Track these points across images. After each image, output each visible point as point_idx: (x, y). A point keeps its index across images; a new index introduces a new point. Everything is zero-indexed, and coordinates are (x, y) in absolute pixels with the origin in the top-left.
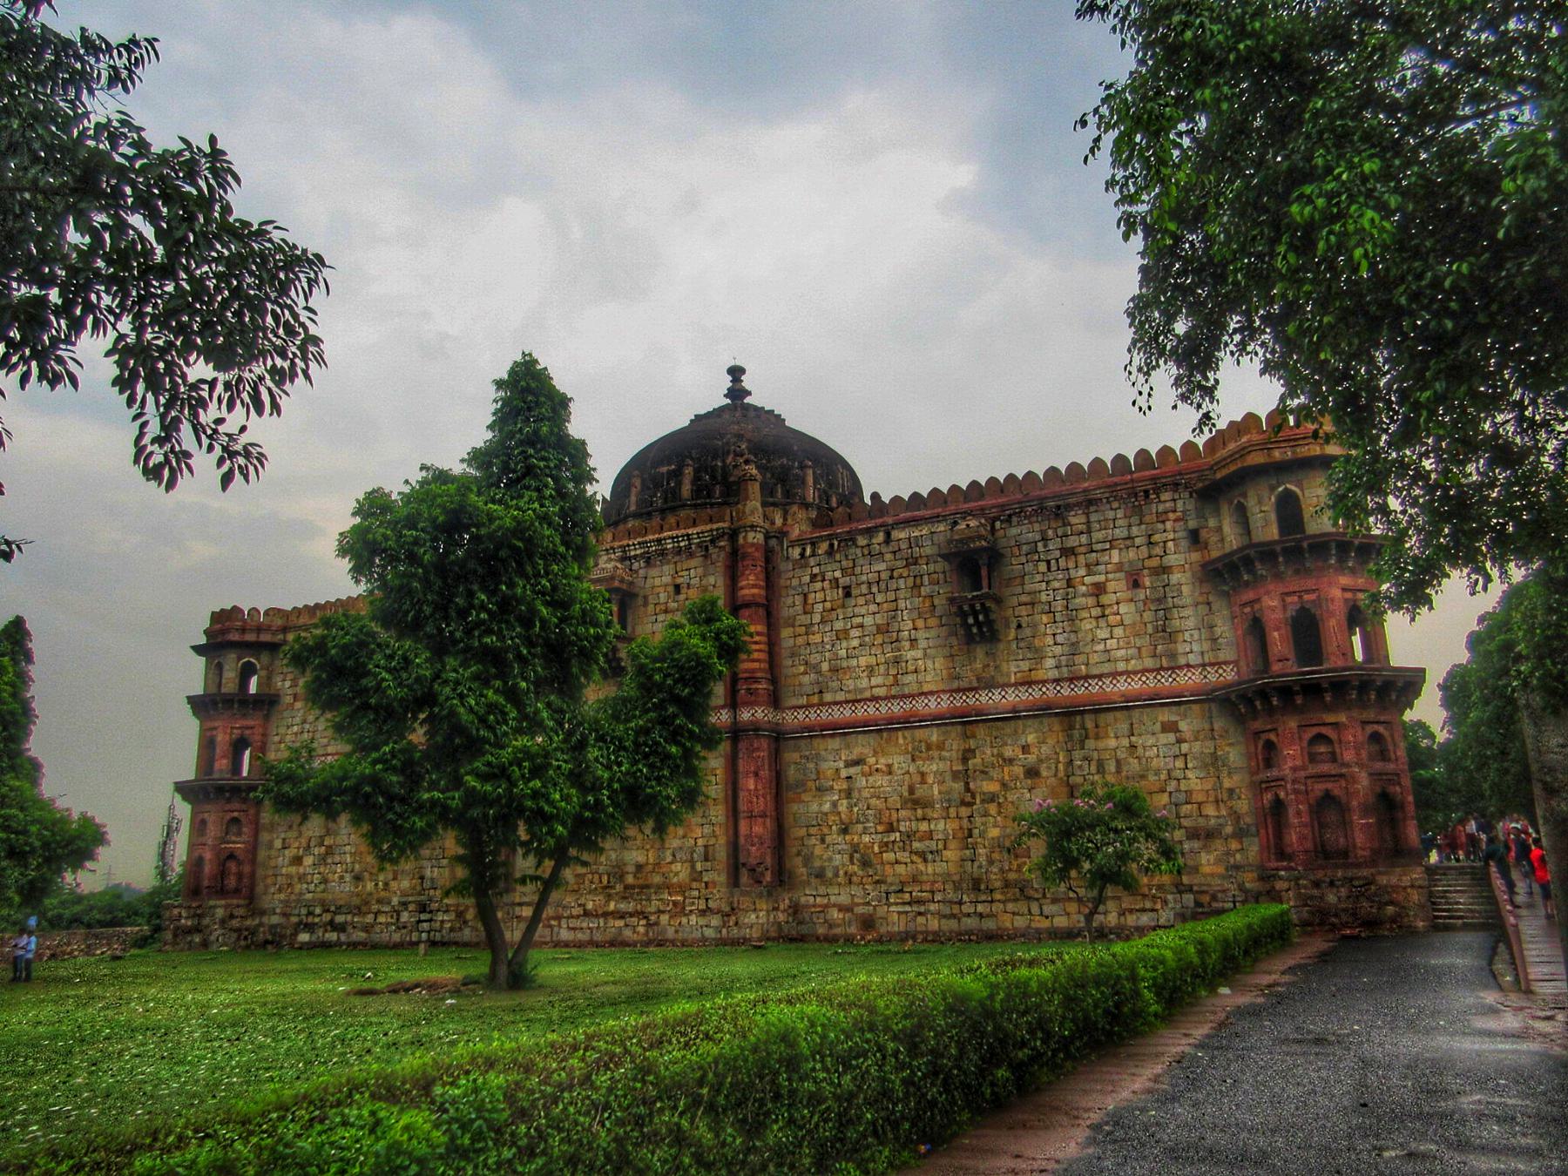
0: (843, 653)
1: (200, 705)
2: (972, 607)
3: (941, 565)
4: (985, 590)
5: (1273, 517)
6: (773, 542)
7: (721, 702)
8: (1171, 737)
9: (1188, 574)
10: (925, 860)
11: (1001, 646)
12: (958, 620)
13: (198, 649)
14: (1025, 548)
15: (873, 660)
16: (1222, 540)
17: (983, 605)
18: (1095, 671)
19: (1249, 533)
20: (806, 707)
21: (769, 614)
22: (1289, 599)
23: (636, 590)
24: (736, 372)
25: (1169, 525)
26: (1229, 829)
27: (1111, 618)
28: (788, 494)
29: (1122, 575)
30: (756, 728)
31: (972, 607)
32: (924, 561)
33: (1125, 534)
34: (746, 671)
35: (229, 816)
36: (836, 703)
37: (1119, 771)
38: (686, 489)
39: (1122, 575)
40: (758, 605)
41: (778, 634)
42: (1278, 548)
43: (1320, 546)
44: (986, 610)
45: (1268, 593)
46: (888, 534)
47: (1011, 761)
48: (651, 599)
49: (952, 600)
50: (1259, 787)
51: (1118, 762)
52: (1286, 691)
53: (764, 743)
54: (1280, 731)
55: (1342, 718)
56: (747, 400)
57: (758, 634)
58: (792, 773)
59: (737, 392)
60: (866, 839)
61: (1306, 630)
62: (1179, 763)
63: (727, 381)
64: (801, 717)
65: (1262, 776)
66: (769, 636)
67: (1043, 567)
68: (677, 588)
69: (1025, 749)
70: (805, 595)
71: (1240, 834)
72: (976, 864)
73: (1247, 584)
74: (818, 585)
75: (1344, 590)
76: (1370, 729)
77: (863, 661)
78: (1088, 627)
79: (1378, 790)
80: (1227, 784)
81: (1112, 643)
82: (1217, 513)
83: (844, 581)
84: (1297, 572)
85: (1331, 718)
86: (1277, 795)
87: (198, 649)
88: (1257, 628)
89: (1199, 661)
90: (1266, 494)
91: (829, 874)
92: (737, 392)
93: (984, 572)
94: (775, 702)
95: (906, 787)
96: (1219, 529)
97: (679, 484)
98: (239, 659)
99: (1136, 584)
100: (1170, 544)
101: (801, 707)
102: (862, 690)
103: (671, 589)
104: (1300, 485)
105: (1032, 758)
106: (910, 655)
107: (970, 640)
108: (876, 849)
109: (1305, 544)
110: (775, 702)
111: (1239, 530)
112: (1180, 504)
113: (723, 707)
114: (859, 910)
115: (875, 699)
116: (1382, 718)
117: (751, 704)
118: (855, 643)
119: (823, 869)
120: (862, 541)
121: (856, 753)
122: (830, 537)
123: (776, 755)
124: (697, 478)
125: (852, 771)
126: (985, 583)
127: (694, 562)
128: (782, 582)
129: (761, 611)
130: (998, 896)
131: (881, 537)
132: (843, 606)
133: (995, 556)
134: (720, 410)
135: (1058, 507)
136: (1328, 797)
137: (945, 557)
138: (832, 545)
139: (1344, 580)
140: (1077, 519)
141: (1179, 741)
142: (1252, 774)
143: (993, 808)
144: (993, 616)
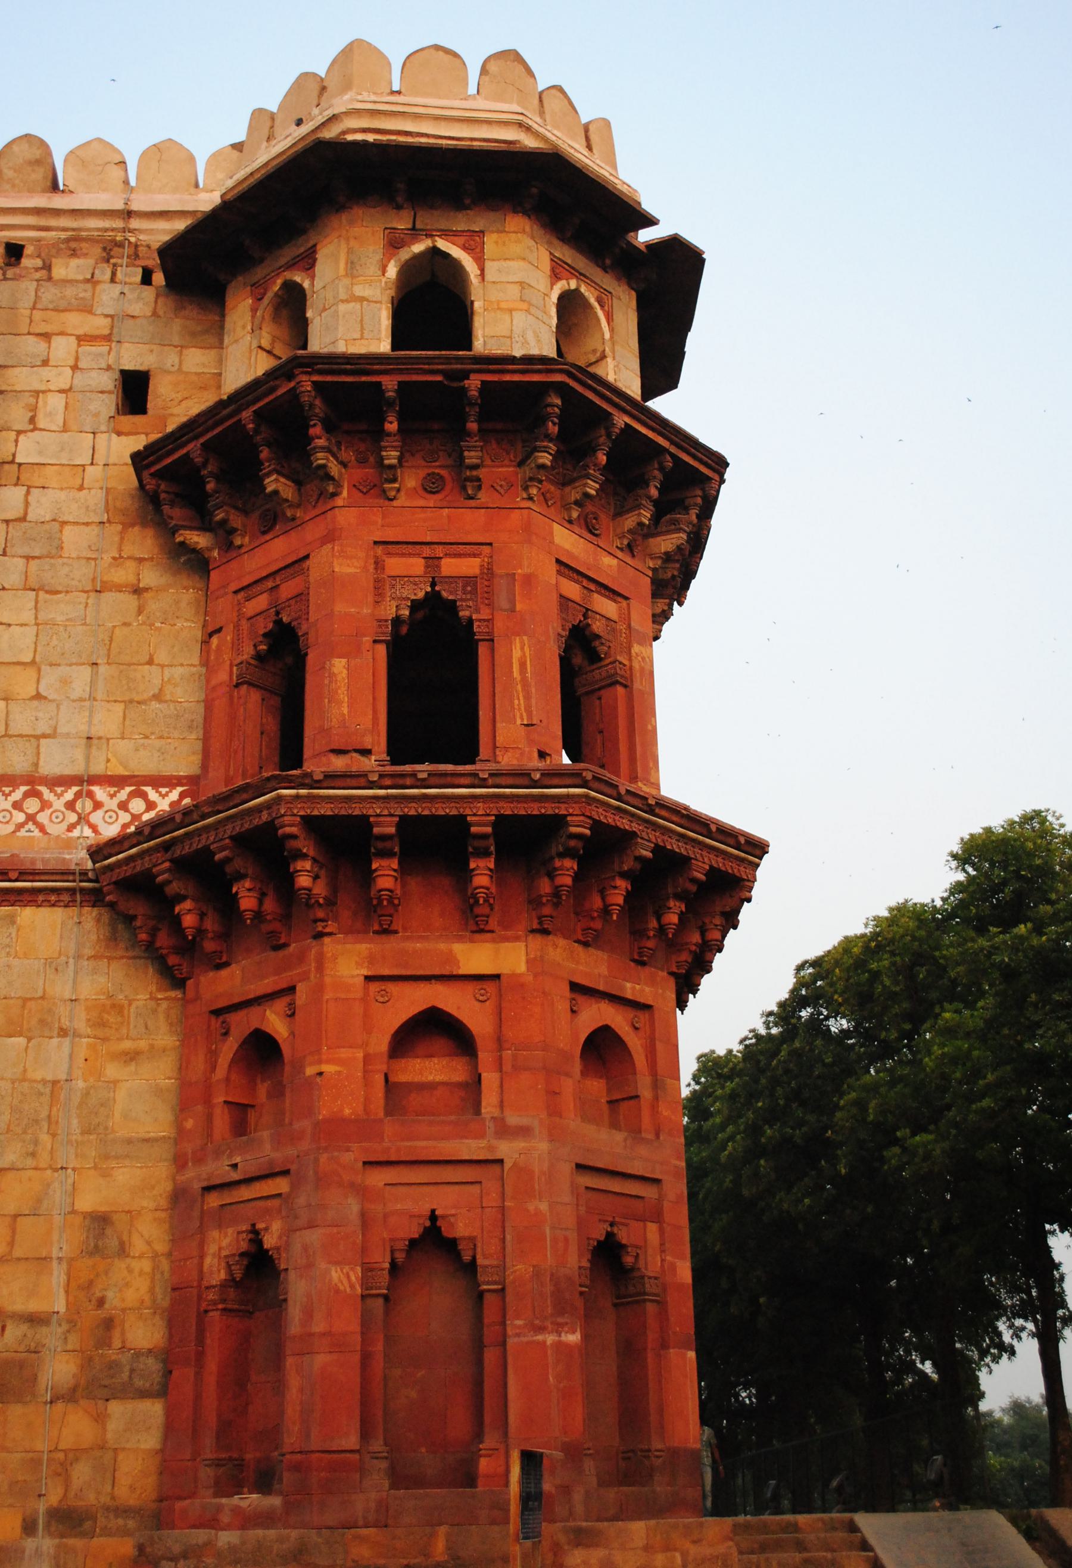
9: (95, 498)
22: (395, 565)
25: (63, 348)
42: (390, 384)
45: (329, 538)
50: (190, 1207)
52: (346, 841)
54: (302, 995)
61: (435, 669)
65: (219, 1169)
71: (98, 1386)
75: (564, 567)
76: (596, 1015)
79: (599, 1232)
84: (432, 486)
85: (476, 957)
86: (255, 1236)
88: (280, 663)
89: (77, 768)
90: (372, 250)
100: (55, 403)
104: (474, 244)
116: (630, 989)
136: (434, 1241)
139: (567, 540)
142: (180, 1162)
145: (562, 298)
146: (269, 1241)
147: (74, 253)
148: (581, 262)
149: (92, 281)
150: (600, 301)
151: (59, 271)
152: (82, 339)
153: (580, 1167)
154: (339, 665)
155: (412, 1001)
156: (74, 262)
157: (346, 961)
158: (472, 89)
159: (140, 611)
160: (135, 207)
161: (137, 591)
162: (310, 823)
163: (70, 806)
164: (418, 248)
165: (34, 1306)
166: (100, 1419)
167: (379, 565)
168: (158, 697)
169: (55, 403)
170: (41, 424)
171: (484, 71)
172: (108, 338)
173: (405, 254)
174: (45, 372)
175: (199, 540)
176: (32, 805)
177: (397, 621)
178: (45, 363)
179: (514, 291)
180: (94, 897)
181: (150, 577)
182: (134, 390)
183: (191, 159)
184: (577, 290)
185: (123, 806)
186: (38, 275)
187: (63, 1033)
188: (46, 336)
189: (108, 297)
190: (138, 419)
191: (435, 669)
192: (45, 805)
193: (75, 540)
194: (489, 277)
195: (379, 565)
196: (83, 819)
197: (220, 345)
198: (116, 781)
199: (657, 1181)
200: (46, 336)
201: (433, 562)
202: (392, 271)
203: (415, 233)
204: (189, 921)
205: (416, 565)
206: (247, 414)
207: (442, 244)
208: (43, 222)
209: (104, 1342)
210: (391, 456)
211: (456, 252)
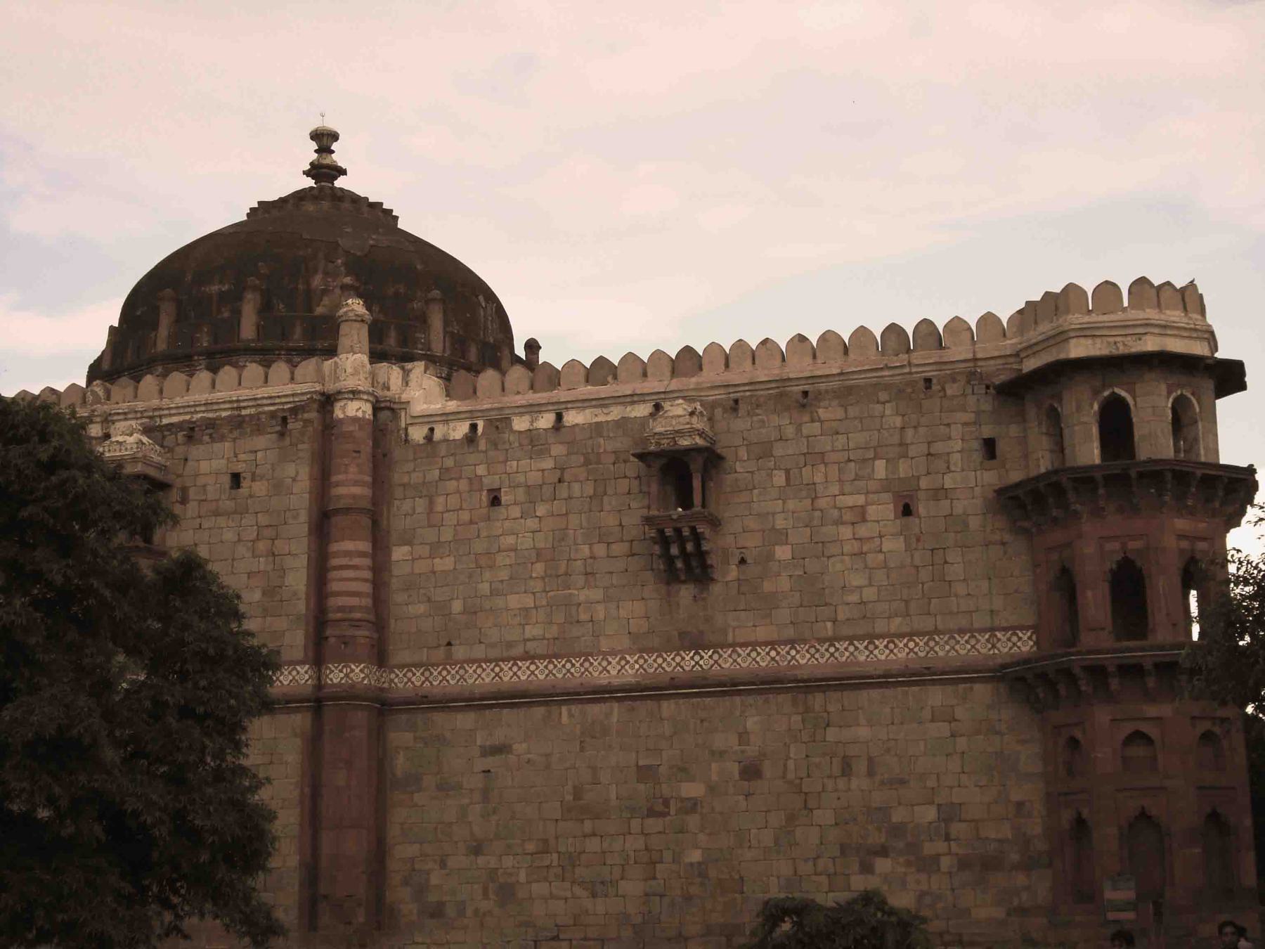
0: (485, 588)
2: (678, 531)
3: (634, 467)
4: (697, 508)
5: (1095, 430)
6: (384, 415)
7: (299, 654)
8: (943, 729)
10: (594, 895)
11: (716, 589)
12: (657, 549)
15: (529, 601)
16: (1026, 456)
17: (693, 529)
18: (846, 631)
19: (1062, 450)
20: (426, 665)
21: (375, 523)
22: (1109, 546)
23: (170, 478)
24: (324, 139)
25: (956, 431)
26: (1015, 857)
27: (870, 557)
28: (404, 340)
29: (887, 497)
30: (349, 695)
31: (678, 531)
32: (612, 458)
33: (896, 439)
34: (341, 609)
36: (473, 661)
37: (871, 773)
38: (248, 329)
39: (887, 497)
40: (360, 511)
41: (389, 555)
43: (1155, 474)
44: (697, 538)
46: (559, 417)
47: (722, 754)
48: (192, 493)
49: (648, 520)
51: (871, 760)
52: (1097, 672)
53: (360, 718)
55: (1164, 710)
56: (340, 183)
57: (362, 554)
58: (400, 764)
59: (324, 172)
60: (508, 862)
61: (1129, 586)
63: (309, 153)
64: (417, 678)
66: (374, 556)
67: (779, 479)
68: (236, 479)
69: (743, 737)
70: (431, 503)
72: (666, 900)
73: (1055, 520)
74: (452, 485)
75: (1181, 537)
76: (1204, 726)
77: (514, 601)
78: (839, 567)
80: (1016, 796)
81: (870, 594)
82: (1022, 418)
83: (491, 482)
85: (1152, 711)
86: (1079, 814)
88: (1066, 585)
89: (988, 625)
91: (450, 911)
92: (324, 172)
93: (697, 483)
94: (380, 657)
95: (569, 788)
96: (1023, 441)
97: (237, 313)
99: (907, 511)
100: (956, 458)
101: (418, 665)
102: (510, 645)
103: (226, 480)
105: (752, 750)
106: (583, 595)
107: (671, 576)
108: (522, 877)
109: (1133, 473)
110: (380, 657)
111: (1045, 442)
113: (302, 663)
115: (530, 657)
117: (344, 659)
118: (504, 574)
119: (441, 905)
121: (499, 736)
122: (471, 414)
123: (378, 735)
124: (265, 309)
125: (490, 762)
126: (697, 498)
127: (261, 441)
128: (398, 477)
129: (366, 521)
131: (546, 421)
132: (489, 519)
133: (712, 459)
134: (299, 197)
135: (805, 393)
136: (1144, 816)
137: (641, 457)
138: (474, 427)
139: (1181, 524)
140: (829, 412)
143: (693, 821)
145: (1176, 401)
146: (1084, 816)
147: (954, 381)
149: (964, 395)
150: (1193, 394)
151: (949, 392)
152: (965, 424)
153: (1200, 788)
154: (1089, 594)
155: (1128, 728)
156: (955, 385)
157: (1102, 715)
158: (1126, 304)
159: (1005, 553)
160: (979, 356)
161: (1003, 544)
162: (1085, 668)
163: (988, 640)
164: (1106, 393)
165: (1000, 836)
168: (1016, 591)
169: (956, 458)
170: (953, 468)
171: (1130, 292)
172: (975, 423)
174: (951, 443)
175: (1026, 524)
176: (973, 642)
178: (950, 438)
179: (1150, 410)
180: (1001, 679)
181: (1007, 537)
182: (990, 447)
183: (999, 320)
184: (1182, 395)
185: (1009, 640)
186: (941, 394)
187: (997, 733)
188: (948, 425)
189: (971, 400)
190: (994, 462)
191: (1129, 586)
192: (978, 641)
193: (974, 523)
194: (1139, 405)
196: (994, 646)
197: (1024, 421)
198: (1005, 629)
199: (1233, 788)
200: (948, 425)
202: (1096, 407)
203: (1104, 387)
204: (1041, 695)
205: (1116, 546)
206: (1041, 485)
207: (1117, 390)
208: (938, 367)
210: (1102, 503)
211: (1123, 394)
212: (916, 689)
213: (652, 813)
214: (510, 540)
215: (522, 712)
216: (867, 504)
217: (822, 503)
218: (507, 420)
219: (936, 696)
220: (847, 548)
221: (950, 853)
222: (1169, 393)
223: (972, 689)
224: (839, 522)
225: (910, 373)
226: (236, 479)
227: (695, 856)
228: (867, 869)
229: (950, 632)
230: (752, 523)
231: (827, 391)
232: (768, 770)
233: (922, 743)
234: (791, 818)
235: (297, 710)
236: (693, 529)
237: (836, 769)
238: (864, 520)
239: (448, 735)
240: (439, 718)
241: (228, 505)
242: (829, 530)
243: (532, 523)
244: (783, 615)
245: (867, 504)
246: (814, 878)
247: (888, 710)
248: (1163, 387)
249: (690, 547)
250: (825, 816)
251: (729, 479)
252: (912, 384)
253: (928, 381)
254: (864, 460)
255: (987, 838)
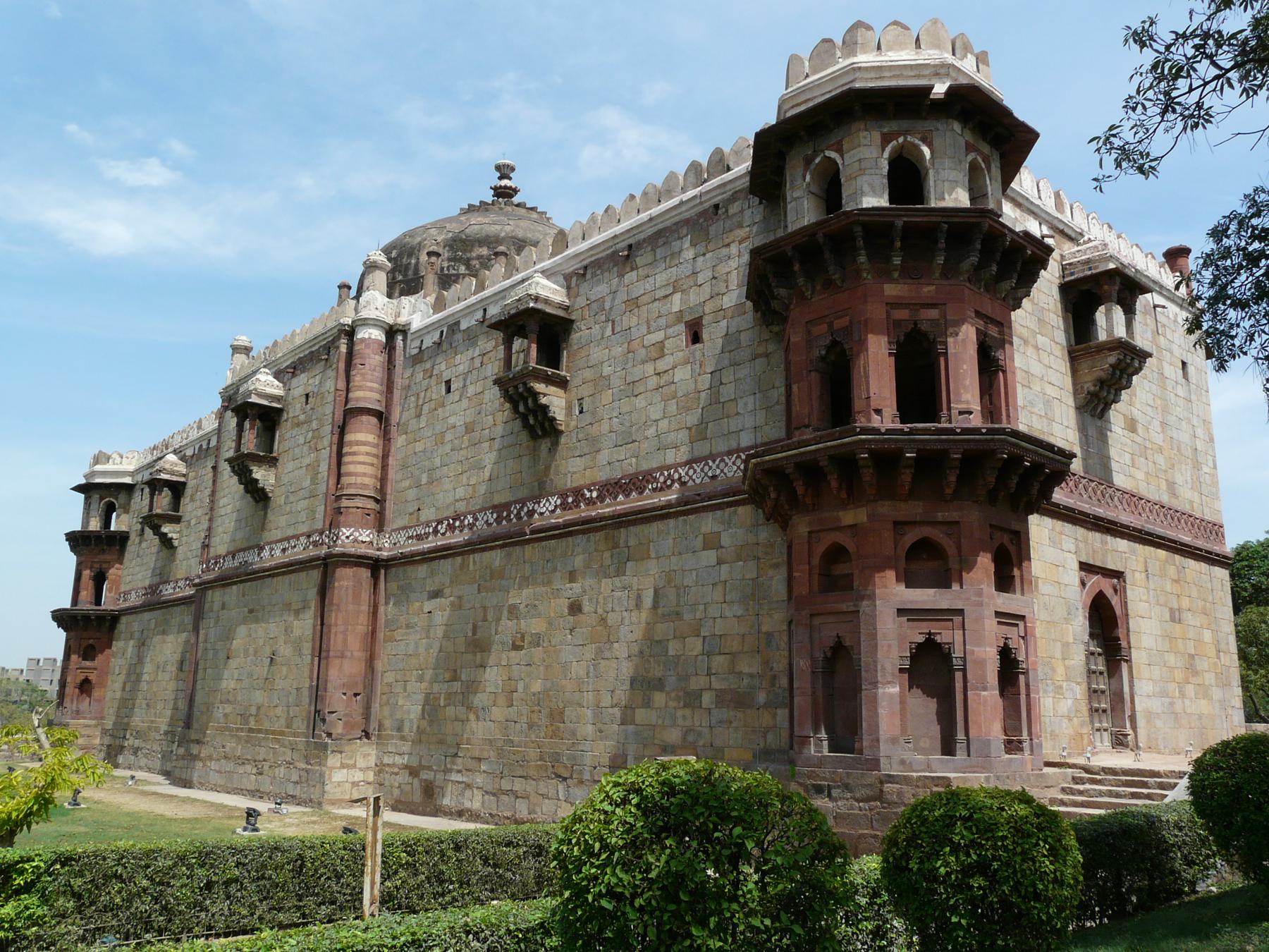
0: (437, 462)
1: (77, 540)
8: (710, 556)
13: (78, 488)
14: (594, 306)
24: (504, 171)
31: (516, 387)
35: (85, 643)
37: (655, 606)
39: (681, 328)
42: (789, 250)
44: (535, 395)
59: (504, 193)
62: (718, 596)
75: (893, 305)
79: (921, 639)
80: (765, 628)
81: (664, 425)
85: (849, 517)
87: (78, 488)
92: (504, 193)
95: (470, 626)
98: (101, 499)
99: (696, 338)
112: (748, 213)
114: (425, 775)
116: (940, 516)
118: (448, 448)
120: (463, 326)
130: (531, 773)
141: (720, 563)
144: (544, 401)
148: (905, 124)
149: (742, 211)
151: (731, 211)
161: (767, 355)
164: (817, 160)
166: (775, 715)
167: (809, 332)
173: (812, 167)
177: (823, 359)
195: (809, 332)
201: (830, 324)
202: (808, 178)
205: (824, 328)
207: (828, 153)
209: (774, 685)
212: (691, 517)
213: (516, 647)
214: (452, 420)
215: (450, 560)
216: (666, 338)
217: (635, 345)
218: (458, 323)
219: (708, 523)
220: (653, 382)
221: (710, 689)
222: (886, 140)
223: (735, 512)
224: (643, 362)
225: (701, 203)
226: (307, 395)
227: (537, 686)
228: (647, 704)
229: (721, 455)
230: (588, 374)
231: (644, 240)
232: (587, 608)
233: (694, 573)
234: (599, 652)
235: (315, 567)
236: (525, 384)
237: (632, 603)
238: (662, 356)
239: (413, 582)
240: (409, 569)
241: (302, 417)
242: (637, 372)
243: (465, 403)
244: (603, 457)
245: (666, 338)
246: (610, 710)
247: (671, 541)
248: (876, 136)
249: (530, 401)
250: (620, 650)
251: (575, 337)
252: (705, 212)
253: (716, 207)
254: (666, 296)
255: (740, 673)
